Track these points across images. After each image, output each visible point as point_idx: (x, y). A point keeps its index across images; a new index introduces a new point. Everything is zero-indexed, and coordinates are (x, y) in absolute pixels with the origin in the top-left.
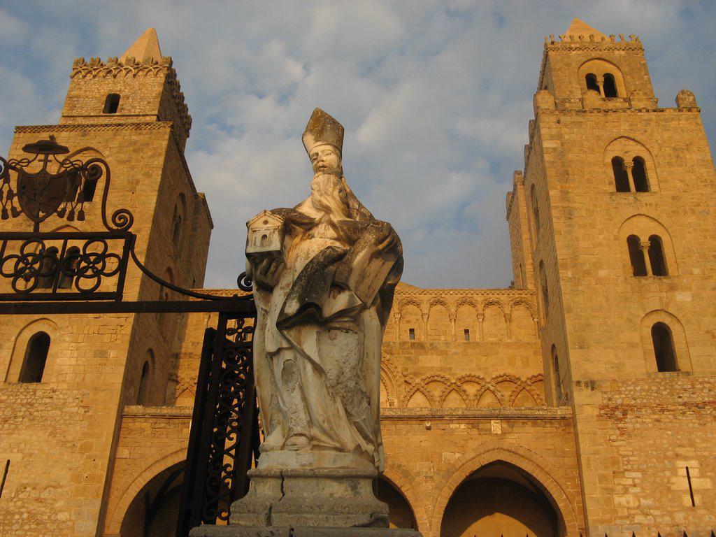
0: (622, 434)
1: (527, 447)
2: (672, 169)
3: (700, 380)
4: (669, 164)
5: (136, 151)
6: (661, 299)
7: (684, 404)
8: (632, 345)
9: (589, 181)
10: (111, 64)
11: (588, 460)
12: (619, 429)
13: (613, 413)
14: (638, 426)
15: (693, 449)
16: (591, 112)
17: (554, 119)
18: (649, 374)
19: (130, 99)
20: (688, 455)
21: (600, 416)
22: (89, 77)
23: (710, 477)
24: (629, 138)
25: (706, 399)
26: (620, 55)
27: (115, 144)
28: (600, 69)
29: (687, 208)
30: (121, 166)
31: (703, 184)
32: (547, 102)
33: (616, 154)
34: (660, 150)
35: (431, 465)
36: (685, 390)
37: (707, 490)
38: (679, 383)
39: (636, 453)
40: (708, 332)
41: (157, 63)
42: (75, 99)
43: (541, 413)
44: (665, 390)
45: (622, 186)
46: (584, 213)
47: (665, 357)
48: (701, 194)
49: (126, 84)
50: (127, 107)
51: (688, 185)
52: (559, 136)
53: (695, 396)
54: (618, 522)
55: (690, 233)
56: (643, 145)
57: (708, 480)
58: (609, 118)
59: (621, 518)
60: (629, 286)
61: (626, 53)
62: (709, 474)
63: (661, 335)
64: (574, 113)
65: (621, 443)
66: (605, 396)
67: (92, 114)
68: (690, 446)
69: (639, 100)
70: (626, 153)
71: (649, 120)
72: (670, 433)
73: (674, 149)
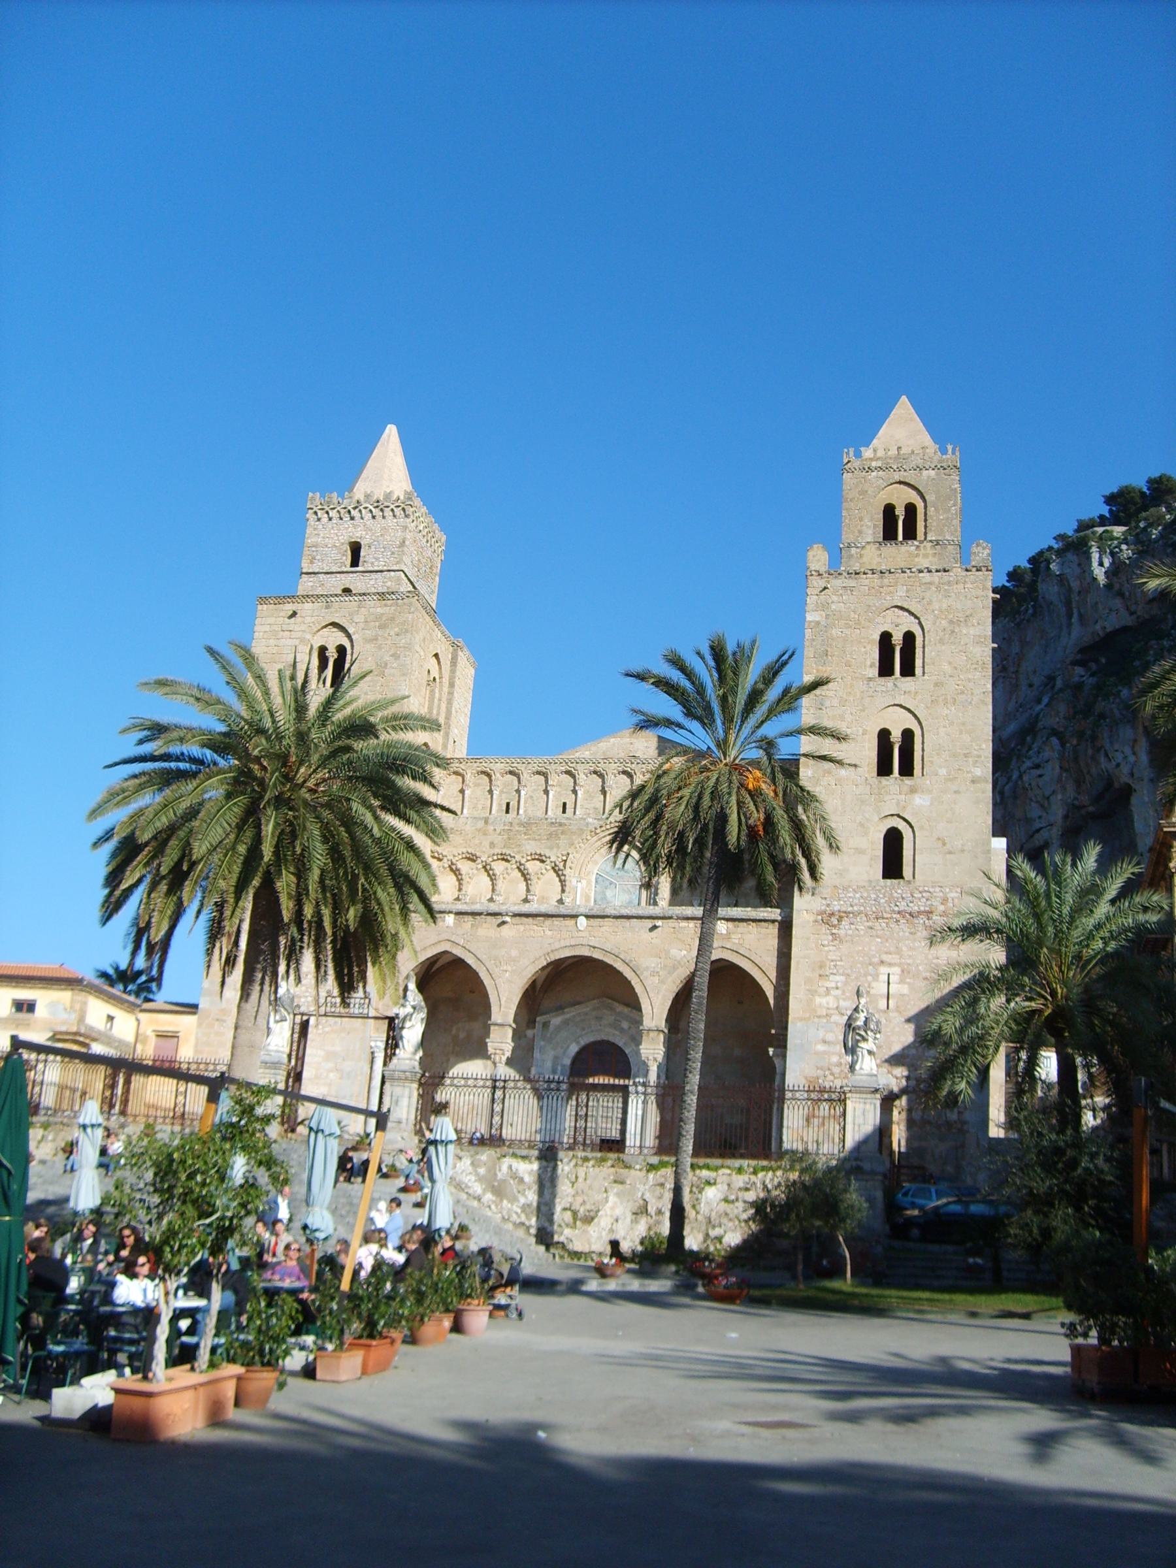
0: (832, 941)
1: (748, 947)
2: (943, 647)
3: (921, 889)
4: (941, 641)
5: (380, 627)
6: (898, 804)
7: (899, 912)
8: (859, 851)
9: (848, 664)
10: (349, 500)
11: (798, 963)
12: (832, 934)
13: (830, 919)
14: (850, 932)
15: (898, 957)
16: (865, 573)
17: (822, 583)
18: (870, 881)
19: (373, 549)
20: (893, 961)
21: (816, 921)
22: (325, 518)
23: (909, 984)
24: (902, 608)
25: (922, 908)
26: (929, 477)
27: (359, 618)
28: (901, 498)
29: (949, 697)
30: (368, 646)
31: (975, 666)
32: (819, 561)
33: (885, 629)
34: (934, 624)
35: (659, 960)
36: (903, 898)
37: (903, 995)
38: (899, 891)
39: (843, 958)
40: (939, 839)
41: (399, 499)
42: (314, 549)
43: (765, 914)
44: (885, 897)
45: (885, 669)
46: (835, 702)
47: (893, 866)
48: (969, 680)
49: (367, 529)
50: (370, 559)
51: (956, 668)
52: (825, 606)
53: (911, 905)
54: (816, 1020)
55: (945, 727)
56: (916, 617)
57: (906, 986)
58: (886, 581)
59: (819, 1017)
60: (869, 787)
61: (937, 474)
62: (908, 980)
63: (893, 842)
64: (845, 574)
65: (831, 948)
66: (824, 902)
67: (334, 569)
68: (895, 953)
69: (926, 556)
70: (896, 626)
71: (930, 583)
72: (879, 940)
73: (951, 622)
